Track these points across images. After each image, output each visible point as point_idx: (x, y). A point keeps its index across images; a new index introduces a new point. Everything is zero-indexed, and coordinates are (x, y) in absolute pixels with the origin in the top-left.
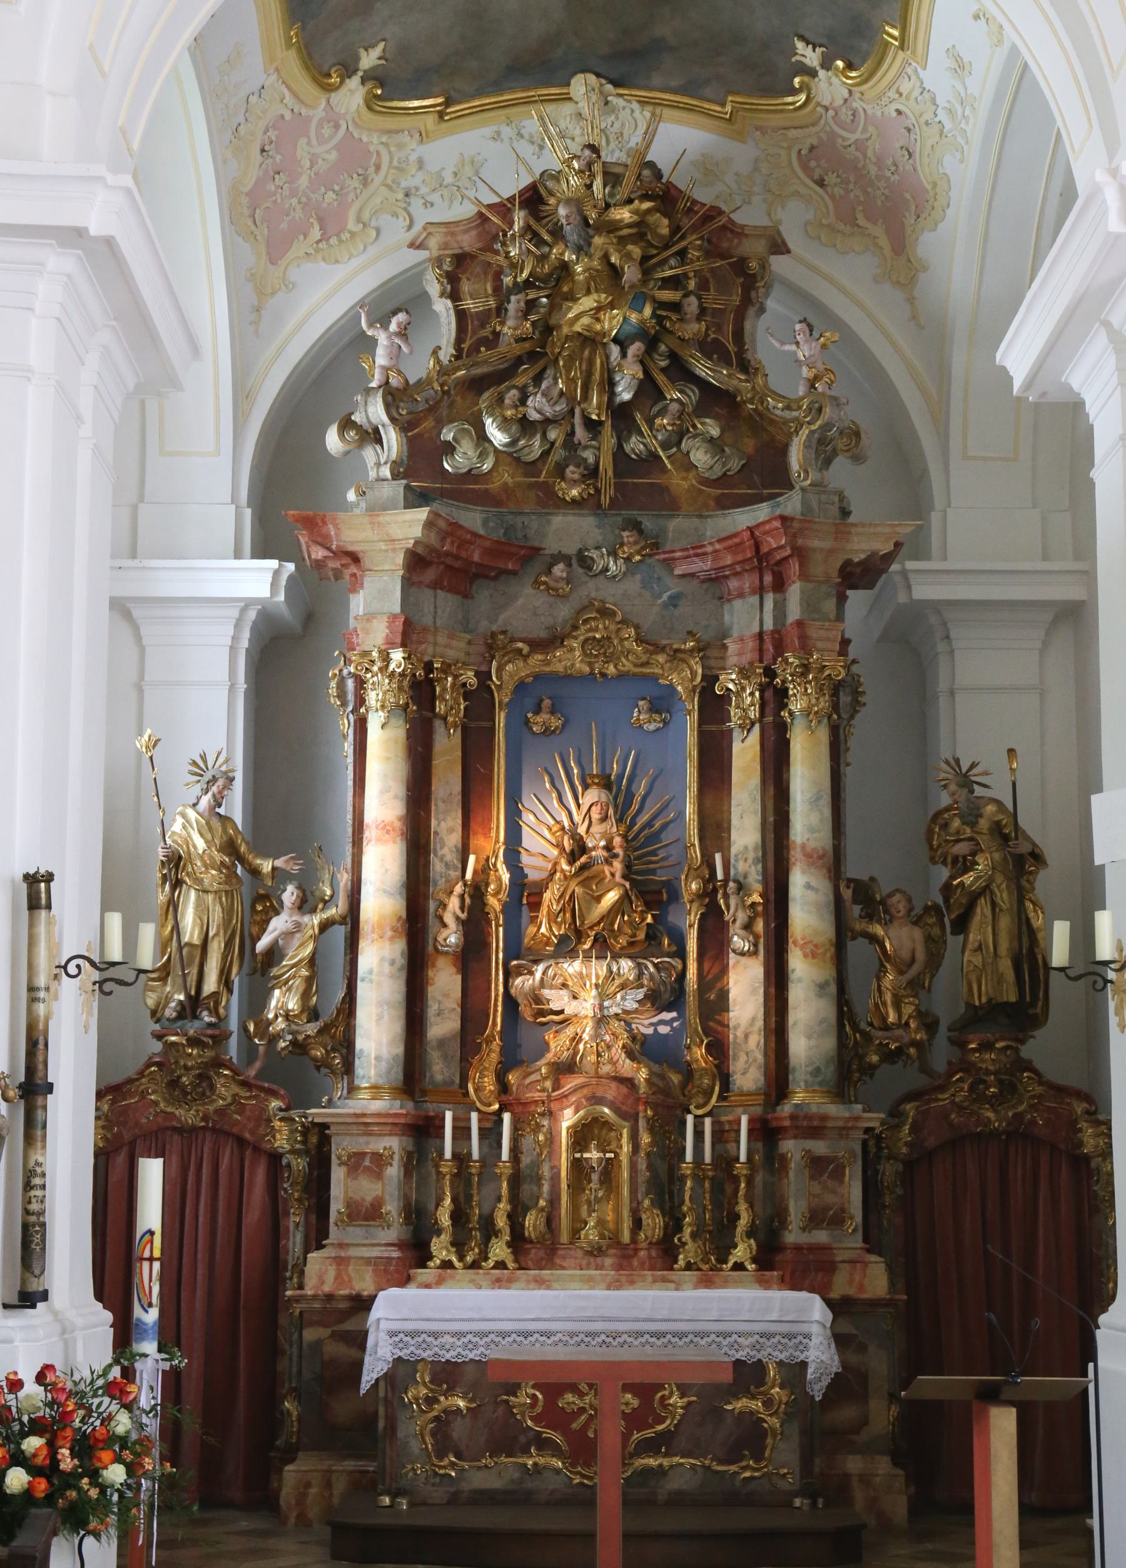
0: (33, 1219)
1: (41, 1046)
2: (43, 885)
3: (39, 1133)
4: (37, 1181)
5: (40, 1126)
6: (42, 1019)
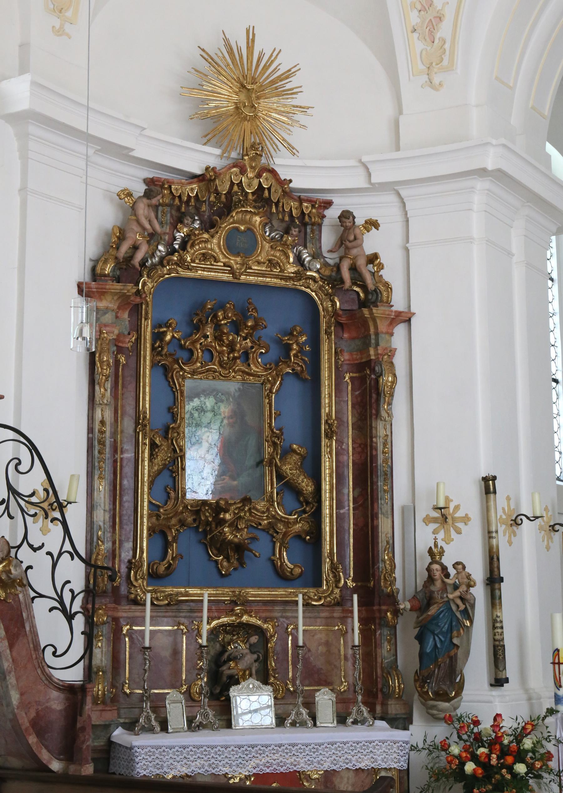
0: (497, 643)
1: (495, 559)
2: (491, 482)
3: (497, 601)
4: (498, 625)
5: (497, 598)
6: (495, 546)
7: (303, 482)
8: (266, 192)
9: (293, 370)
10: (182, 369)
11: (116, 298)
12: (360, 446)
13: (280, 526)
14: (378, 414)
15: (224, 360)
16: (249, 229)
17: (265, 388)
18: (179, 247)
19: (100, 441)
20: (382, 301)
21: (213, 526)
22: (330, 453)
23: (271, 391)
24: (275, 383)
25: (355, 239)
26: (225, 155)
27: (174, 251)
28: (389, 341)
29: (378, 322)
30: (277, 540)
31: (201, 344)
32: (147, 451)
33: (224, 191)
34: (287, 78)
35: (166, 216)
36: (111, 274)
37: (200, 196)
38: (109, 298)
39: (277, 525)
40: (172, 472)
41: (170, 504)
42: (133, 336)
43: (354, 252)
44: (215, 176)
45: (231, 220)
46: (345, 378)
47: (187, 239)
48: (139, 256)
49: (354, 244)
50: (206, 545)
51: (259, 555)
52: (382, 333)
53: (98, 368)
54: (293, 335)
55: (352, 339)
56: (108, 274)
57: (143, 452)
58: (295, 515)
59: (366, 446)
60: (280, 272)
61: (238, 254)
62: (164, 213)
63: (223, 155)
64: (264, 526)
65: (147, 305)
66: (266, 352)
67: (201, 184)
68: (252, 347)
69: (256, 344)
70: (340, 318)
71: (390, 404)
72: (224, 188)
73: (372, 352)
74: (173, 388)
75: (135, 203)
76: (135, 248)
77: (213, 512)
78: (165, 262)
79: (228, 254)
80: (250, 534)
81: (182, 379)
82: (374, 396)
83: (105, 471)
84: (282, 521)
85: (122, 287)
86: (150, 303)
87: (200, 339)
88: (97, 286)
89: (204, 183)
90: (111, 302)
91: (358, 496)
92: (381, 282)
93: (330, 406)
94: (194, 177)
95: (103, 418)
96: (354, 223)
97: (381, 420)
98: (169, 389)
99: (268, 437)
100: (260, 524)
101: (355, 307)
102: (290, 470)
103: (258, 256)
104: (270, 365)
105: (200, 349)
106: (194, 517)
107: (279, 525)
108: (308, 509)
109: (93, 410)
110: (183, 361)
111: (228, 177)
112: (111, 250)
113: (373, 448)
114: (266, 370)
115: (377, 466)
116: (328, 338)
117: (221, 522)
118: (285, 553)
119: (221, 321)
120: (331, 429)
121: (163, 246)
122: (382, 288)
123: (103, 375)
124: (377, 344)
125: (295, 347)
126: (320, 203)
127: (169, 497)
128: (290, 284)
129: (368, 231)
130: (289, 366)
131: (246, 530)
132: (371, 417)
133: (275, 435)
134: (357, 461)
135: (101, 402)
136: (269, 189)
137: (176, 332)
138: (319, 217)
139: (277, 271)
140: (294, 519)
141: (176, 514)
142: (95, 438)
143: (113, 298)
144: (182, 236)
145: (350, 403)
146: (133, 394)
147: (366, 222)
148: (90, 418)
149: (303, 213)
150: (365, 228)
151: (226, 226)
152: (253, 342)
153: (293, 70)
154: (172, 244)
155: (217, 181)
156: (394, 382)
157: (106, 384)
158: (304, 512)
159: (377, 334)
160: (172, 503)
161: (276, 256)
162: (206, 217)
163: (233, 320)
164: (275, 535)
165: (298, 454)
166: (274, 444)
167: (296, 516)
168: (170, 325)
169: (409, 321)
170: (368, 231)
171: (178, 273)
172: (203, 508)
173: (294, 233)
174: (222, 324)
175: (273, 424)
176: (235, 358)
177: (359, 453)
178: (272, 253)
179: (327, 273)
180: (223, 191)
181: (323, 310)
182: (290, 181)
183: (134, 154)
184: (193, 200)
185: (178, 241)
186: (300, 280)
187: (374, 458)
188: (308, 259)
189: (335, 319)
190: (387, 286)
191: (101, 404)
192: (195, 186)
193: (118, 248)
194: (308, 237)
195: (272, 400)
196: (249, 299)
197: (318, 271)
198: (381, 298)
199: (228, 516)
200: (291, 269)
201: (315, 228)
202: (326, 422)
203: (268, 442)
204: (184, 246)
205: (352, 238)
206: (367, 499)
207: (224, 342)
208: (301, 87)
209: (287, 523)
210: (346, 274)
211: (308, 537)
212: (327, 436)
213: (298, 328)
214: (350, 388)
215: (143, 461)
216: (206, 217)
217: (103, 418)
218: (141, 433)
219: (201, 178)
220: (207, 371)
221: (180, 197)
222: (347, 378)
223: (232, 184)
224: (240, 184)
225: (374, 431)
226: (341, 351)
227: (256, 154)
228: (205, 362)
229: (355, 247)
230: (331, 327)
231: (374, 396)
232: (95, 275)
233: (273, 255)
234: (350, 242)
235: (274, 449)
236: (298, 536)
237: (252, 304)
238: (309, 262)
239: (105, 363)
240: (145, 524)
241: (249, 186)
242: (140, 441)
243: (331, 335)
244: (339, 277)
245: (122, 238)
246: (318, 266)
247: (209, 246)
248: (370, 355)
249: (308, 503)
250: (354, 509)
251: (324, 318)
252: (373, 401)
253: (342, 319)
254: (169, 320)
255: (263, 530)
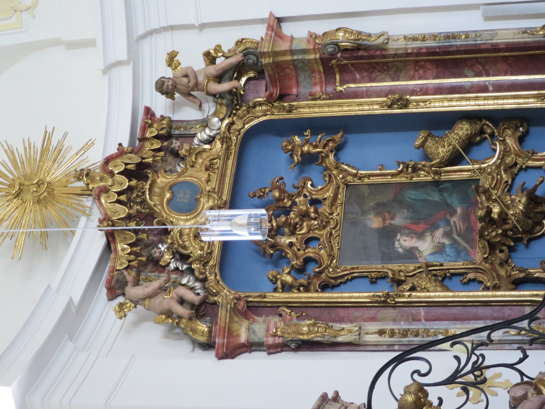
7: (457, 134)
8: (129, 167)
9: (332, 151)
10: (327, 268)
11: (236, 319)
12: (416, 71)
13: (508, 160)
14: (381, 48)
15: (318, 224)
16: (170, 188)
17: (351, 182)
18: (186, 264)
19: (403, 334)
20: (256, 48)
21: (507, 227)
22: (424, 101)
23: (355, 175)
24: (346, 170)
25: (186, 76)
26: (87, 212)
27: (191, 271)
28: (301, 40)
29: (277, 49)
30: (524, 164)
31: (299, 250)
32: (418, 294)
33: (125, 210)
34: (13, 153)
35: (150, 277)
36: (209, 325)
37: (131, 242)
38: (235, 326)
39: (507, 164)
40: (444, 278)
41: (480, 277)
42: (284, 311)
43: (201, 78)
44: (108, 220)
45: (159, 207)
46: (341, 91)
47: (178, 256)
48: (189, 295)
49: (191, 76)
50: (530, 240)
51: (541, 177)
52: (291, 46)
53: (317, 337)
54: (292, 150)
55: (298, 84)
56: (209, 327)
57: (419, 297)
58: (496, 145)
59: (417, 62)
60: (220, 160)
61: (197, 200)
62: (146, 279)
63: (87, 214)
64: (508, 178)
65: (251, 296)
66: (311, 180)
67: (118, 241)
68: (305, 196)
69: (302, 192)
70: (274, 95)
71: (370, 35)
72: (122, 211)
73: (312, 57)
74: (347, 279)
75: (131, 301)
76: (182, 301)
77: (492, 226)
78: (201, 277)
79: (196, 211)
80: (517, 193)
81: (338, 268)
82: (361, 53)
83: (439, 329)
84: (503, 158)
85: (224, 309)
86: (247, 294)
87: (293, 250)
88: (221, 337)
89: (116, 236)
90: (241, 325)
91: (474, 71)
92: (235, 50)
93: (372, 104)
94: (109, 248)
95: (376, 333)
96: (170, 78)
97: (387, 43)
98: (349, 283)
99: (407, 178)
100: (507, 182)
101: (263, 83)
102: (444, 147)
103: (200, 179)
104: (325, 176)
105: (304, 250)
106: (498, 251)
107: (507, 161)
108: (489, 131)
109: (367, 345)
110: (318, 266)
111: (110, 206)
112: (182, 326)
113: (418, 53)
114: (330, 181)
115: (439, 47)
116: (296, 108)
117: (503, 217)
118: (540, 154)
119: (272, 225)
120: (398, 100)
121: (183, 279)
122: (241, 48)
123: (325, 331)
124: (304, 51)
125: (306, 148)
126: (147, 118)
127: (474, 280)
128: (234, 150)
129: (180, 64)
130: (327, 156)
131: (513, 197)
132: (384, 56)
133: (405, 169)
134: (434, 75)
135: (357, 333)
136: (126, 164)
137: (283, 271)
138: (163, 120)
139: (218, 163)
140: (500, 144)
141: (493, 269)
142: (399, 341)
143: (237, 322)
144: (174, 261)
145: (369, 85)
146: (351, 310)
147: (170, 65)
148: (376, 349)
149: (157, 137)
150: (176, 67)
151: (165, 212)
152: (299, 195)
153: (6, 148)
154: (182, 271)
155: (114, 218)
156: (346, 30)
157: (336, 329)
158: (492, 135)
159: (292, 52)
160: (481, 275)
161: (202, 163)
162: (155, 239)
163: (272, 214)
164: (518, 166)
165: (426, 140)
166: (415, 169)
167: (498, 144)
168: (275, 277)
169: (280, 20)
170: (180, 64)
171: (215, 265)
172: (486, 238)
173: (178, 144)
174: (277, 225)
175: (393, 171)
176: (316, 212)
177: (425, 72)
178: (198, 166)
179: (224, 110)
180: (125, 212)
181: (266, 115)
182: (120, 145)
183: (77, 299)
184: (135, 249)
185: (179, 265)
186: (230, 138)
187: (431, 52)
188: (207, 131)
189: (275, 102)
190: (239, 43)
191: (359, 334)
192: (119, 245)
193: (180, 317)
194: (184, 133)
195: (365, 174)
196: (249, 196)
197: (222, 120)
198: (252, 49)
199: (496, 210)
200: (218, 144)
201: (174, 126)
202: (390, 107)
203: (412, 177)
204: (184, 258)
205: (185, 80)
206: (476, 58)
207: (297, 224)
208: (24, 140)
209: (505, 153)
210: (225, 86)
211: (521, 129)
212: (406, 106)
213: (284, 144)
214: (352, 85)
215: (429, 297)
216: (155, 239)
217: (376, 333)
218: (397, 300)
219: (110, 239)
220: (330, 242)
221: (130, 261)
222: (341, 89)
223: (118, 202)
224: (119, 193)
225: (400, 52)
226: (310, 95)
227: (87, 175)
228: (320, 245)
229: (196, 77)
230: (283, 106)
231: (361, 53)
232: (207, 346)
233: (201, 166)
234: (189, 82)
235: (421, 169)
236: (521, 140)
237: (255, 192)
238: (211, 130)
239: (311, 329)
240: (503, 293)
241: (121, 184)
242: (406, 300)
243: (293, 106)
244: (228, 96)
245: (169, 314)
246: (216, 119)
247: (187, 231)
248: (315, 59)
249: (482, 132)
250: (488, 75)
251: (273, 115)
252: (366, 54)
253: (275, 92)
254: (269, 278)
255: (513, 180)
